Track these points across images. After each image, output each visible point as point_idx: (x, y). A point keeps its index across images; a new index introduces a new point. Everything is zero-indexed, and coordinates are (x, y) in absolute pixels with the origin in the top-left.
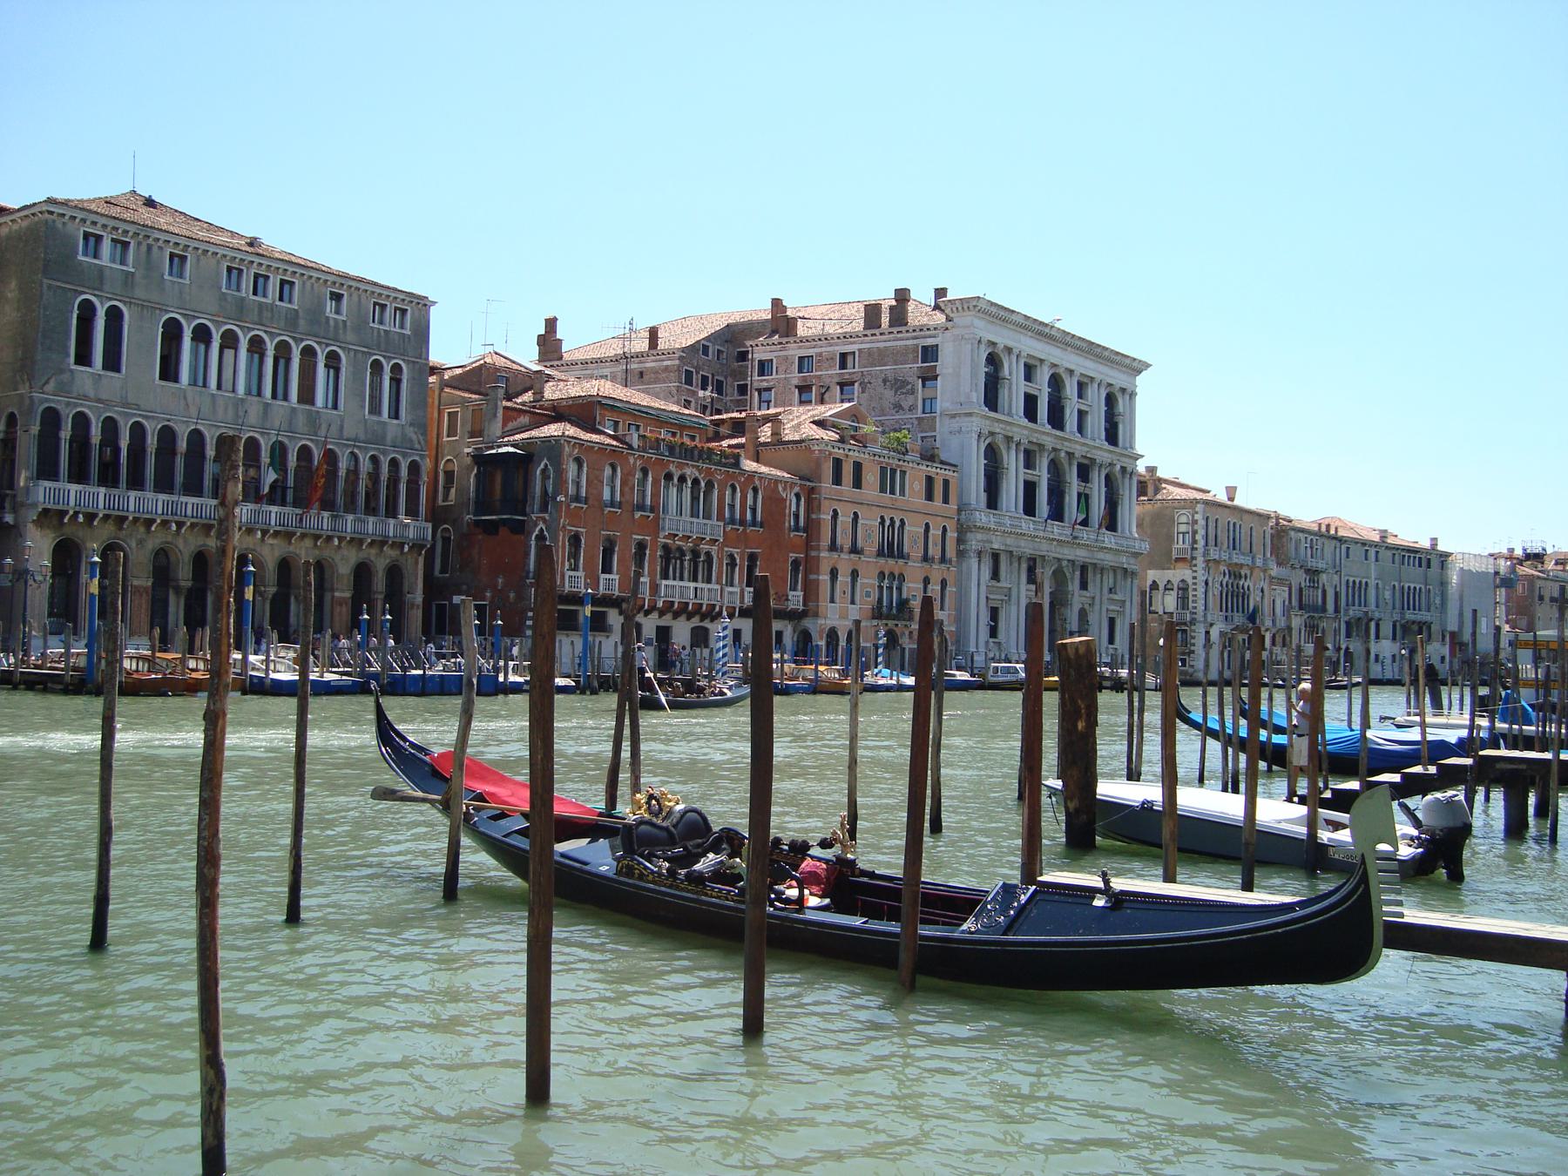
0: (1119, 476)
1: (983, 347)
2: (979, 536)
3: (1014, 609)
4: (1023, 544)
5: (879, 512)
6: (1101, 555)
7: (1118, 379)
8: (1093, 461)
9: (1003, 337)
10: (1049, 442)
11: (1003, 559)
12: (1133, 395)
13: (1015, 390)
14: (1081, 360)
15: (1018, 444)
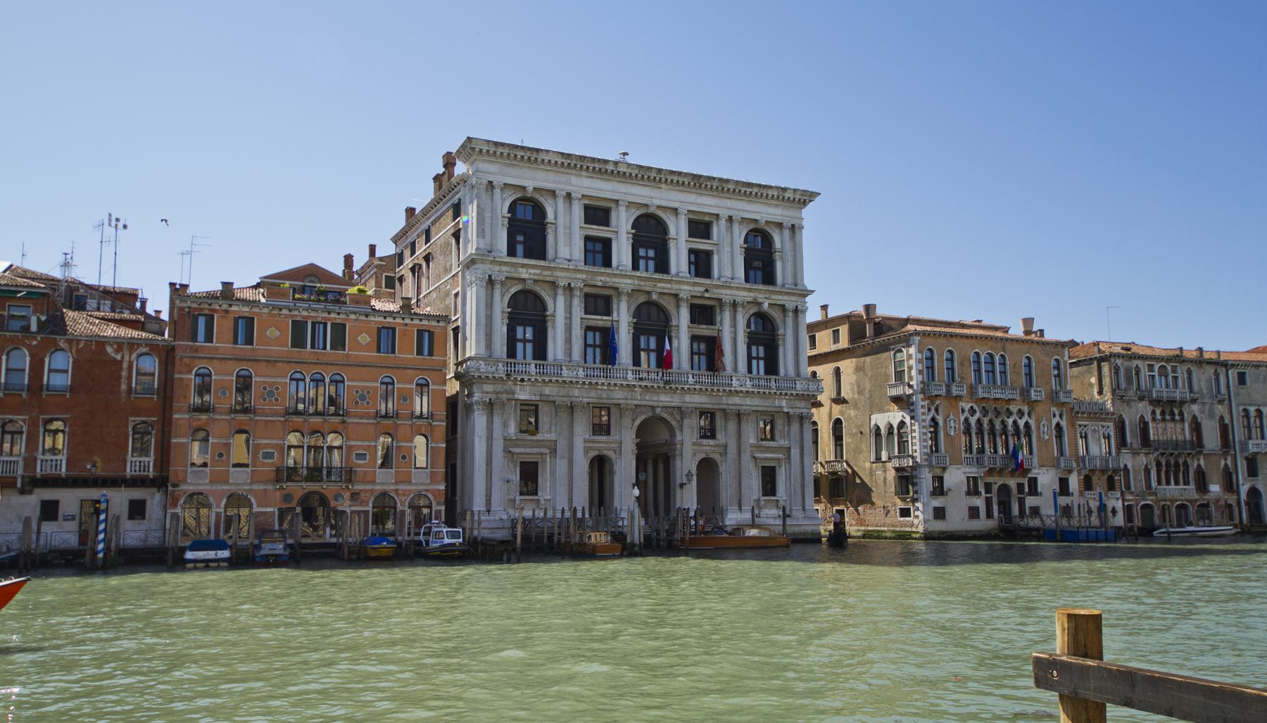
0: (776, 314)
1: (497, 191)
2: (488, 388)
3: (561, 465)
4: (576, 392)
5: (236, 368)
6: (736, 400)
7: (764, 212)
8: (720, 300)
9: (531, 179)
10: (626, 284)
11: (544, 410)
12: (794, 229)
13: (567, 237)
14: (691, 198)
15: (569, 289)
